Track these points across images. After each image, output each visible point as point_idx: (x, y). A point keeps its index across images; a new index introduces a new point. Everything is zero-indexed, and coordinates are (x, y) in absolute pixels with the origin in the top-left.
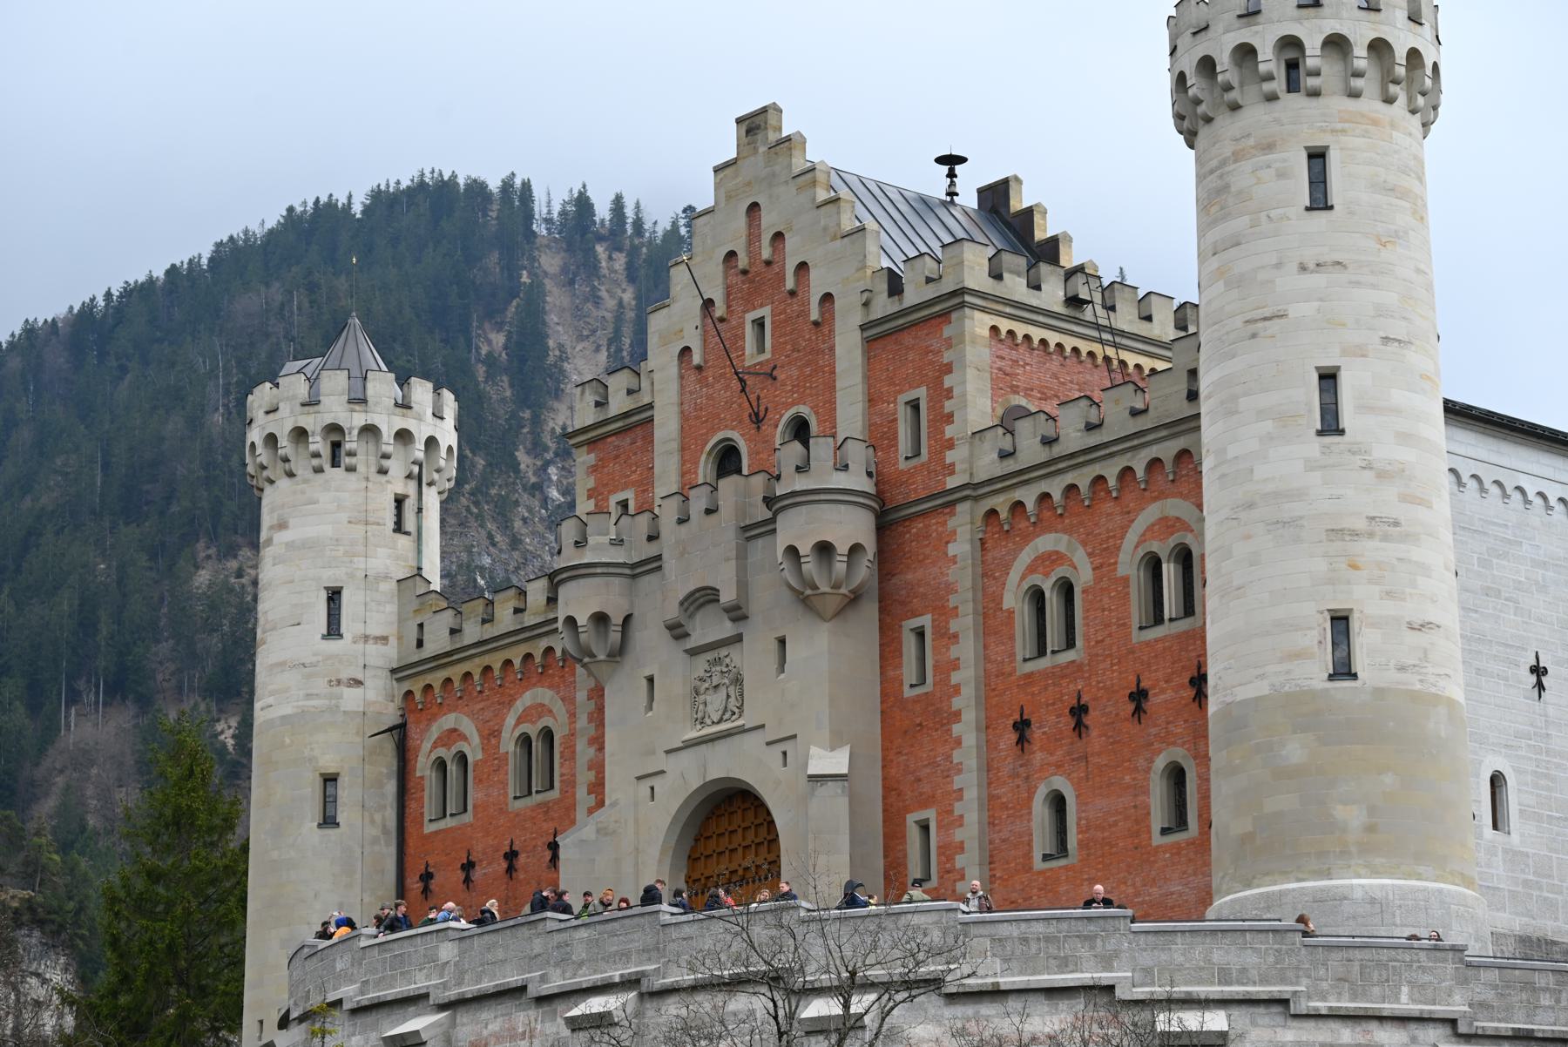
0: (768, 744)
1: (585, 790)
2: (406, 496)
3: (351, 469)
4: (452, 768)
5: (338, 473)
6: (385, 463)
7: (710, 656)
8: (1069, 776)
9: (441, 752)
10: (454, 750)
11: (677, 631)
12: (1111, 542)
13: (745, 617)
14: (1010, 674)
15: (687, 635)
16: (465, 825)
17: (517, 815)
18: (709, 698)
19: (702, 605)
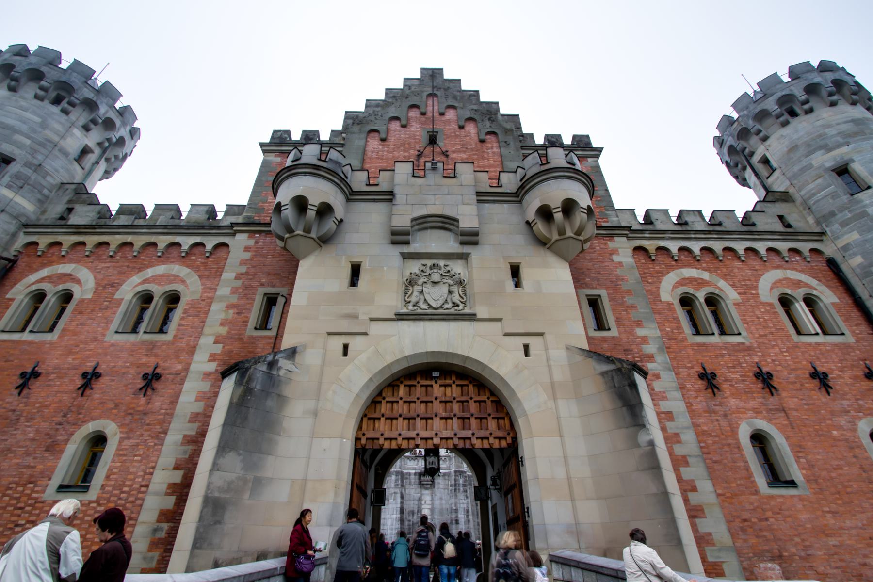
0: (506, 334)
1: (212, 339)
2: (92, 151)
3: (65, 112)
4: (51, 300)
5: (56, 109)
6: (92, 126)
7: (429, 263)
8: (770, 421)
9: (46, 286)
10: (60, 287)
11: (399, 238)
12: (748, 283)
13: (476, 243)
14: (683, 341)
15: (407, 243)
16: (43, 343)
17: (113, 345)
18: (425, 289)
19: (426, 229)
